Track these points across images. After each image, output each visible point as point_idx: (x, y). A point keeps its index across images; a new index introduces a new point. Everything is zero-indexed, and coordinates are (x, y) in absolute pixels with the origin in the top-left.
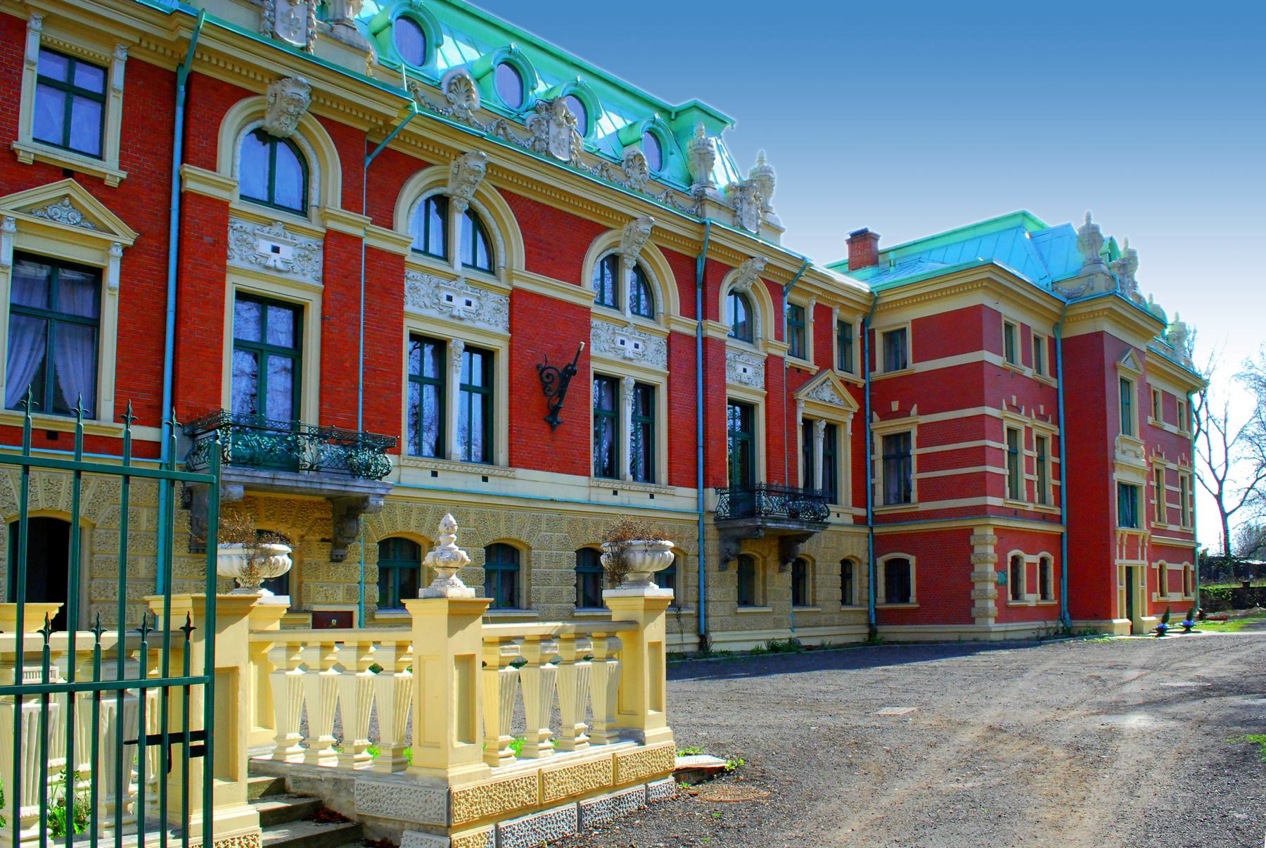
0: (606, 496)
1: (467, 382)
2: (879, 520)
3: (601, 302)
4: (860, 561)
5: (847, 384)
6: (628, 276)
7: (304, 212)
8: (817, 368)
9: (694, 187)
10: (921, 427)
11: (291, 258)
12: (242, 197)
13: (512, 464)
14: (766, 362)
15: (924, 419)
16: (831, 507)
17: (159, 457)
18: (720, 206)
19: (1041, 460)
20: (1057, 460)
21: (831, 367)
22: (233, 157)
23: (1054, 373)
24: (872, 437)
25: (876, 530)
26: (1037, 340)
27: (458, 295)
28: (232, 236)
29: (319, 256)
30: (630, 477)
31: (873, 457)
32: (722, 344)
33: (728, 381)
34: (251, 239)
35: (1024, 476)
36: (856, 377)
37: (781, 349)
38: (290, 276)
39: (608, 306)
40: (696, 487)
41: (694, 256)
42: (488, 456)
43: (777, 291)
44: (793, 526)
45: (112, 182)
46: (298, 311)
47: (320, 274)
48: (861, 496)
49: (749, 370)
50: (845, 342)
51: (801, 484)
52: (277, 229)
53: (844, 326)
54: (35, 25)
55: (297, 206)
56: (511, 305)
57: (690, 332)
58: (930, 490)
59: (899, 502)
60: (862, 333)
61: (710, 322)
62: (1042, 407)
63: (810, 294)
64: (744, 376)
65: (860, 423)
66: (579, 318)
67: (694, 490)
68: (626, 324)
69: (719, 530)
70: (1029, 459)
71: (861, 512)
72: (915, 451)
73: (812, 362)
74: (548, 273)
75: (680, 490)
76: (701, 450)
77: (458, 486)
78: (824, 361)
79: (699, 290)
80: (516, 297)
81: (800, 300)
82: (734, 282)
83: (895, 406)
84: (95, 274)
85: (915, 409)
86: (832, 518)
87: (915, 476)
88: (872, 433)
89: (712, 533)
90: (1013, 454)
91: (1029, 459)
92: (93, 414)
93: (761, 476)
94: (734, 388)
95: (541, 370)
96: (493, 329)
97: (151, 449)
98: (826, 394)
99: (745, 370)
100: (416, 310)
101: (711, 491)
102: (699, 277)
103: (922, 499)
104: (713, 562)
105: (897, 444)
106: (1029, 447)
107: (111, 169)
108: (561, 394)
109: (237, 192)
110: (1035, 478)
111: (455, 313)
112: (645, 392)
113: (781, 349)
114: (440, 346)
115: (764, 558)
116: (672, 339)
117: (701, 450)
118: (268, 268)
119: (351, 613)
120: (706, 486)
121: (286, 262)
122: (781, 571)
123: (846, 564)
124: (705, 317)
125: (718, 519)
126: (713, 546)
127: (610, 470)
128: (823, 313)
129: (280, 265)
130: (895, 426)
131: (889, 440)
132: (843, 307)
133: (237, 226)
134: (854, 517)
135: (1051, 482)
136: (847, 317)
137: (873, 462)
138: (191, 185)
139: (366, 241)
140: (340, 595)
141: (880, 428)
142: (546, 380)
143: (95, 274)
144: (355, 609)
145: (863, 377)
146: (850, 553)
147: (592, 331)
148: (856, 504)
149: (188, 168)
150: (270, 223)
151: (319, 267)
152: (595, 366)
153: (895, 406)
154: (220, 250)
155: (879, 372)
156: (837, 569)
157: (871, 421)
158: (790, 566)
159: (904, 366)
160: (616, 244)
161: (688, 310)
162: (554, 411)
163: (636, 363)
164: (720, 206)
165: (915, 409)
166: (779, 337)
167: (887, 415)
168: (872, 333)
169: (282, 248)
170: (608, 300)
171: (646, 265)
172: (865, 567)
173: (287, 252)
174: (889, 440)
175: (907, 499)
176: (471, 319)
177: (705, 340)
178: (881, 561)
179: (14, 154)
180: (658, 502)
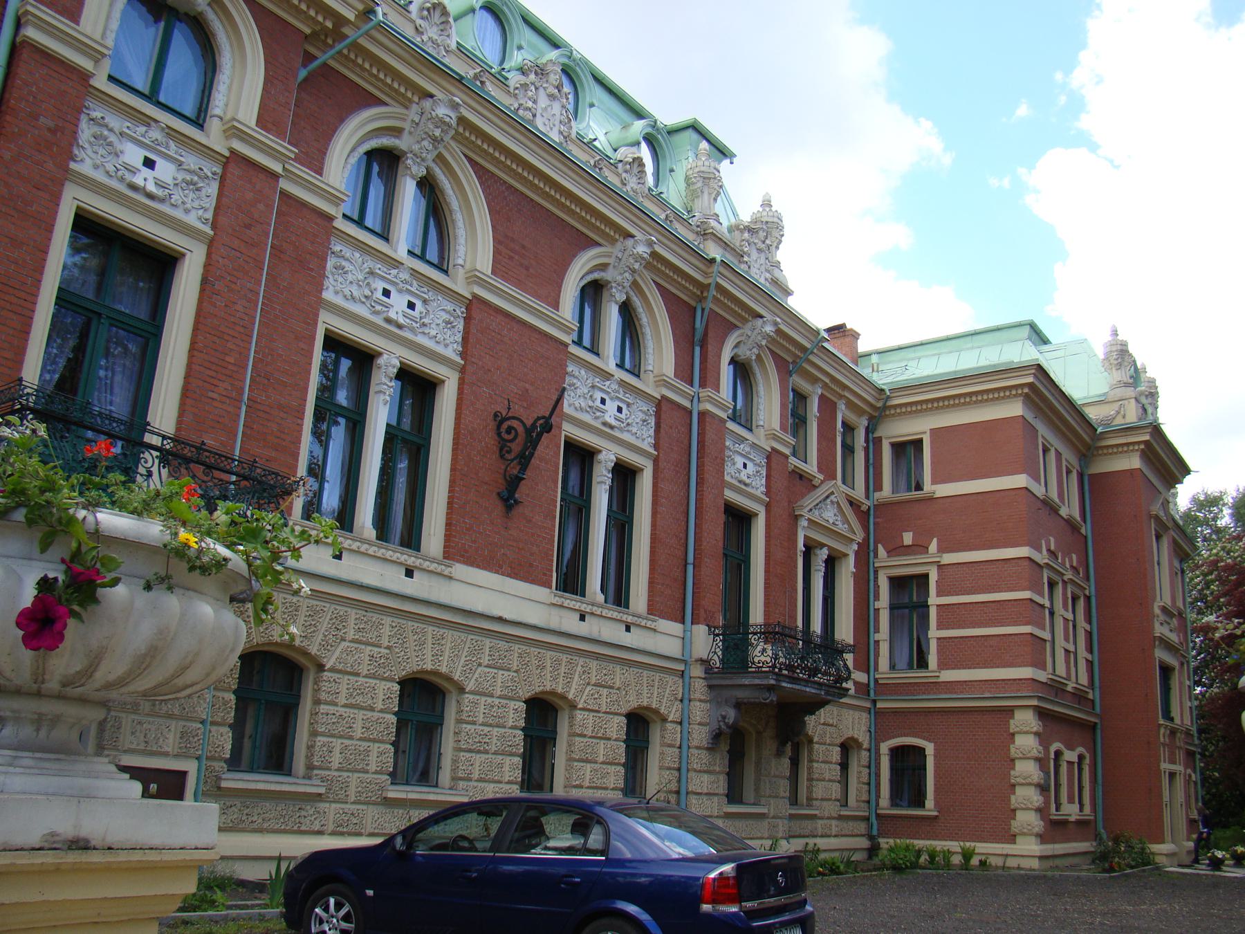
0: (570, 623)
1: (394, 423)
3: (579, 343)
5: (852, 503)
7: (198, 121)
8: (821, 477)
11: (170, 181)
12: (111, 78)
15: (948, 558)
20: (1088, 627)
21: (834, 478)
22: (108, 17)
24: (876, 578)
25: (879, 705)
26: (1069, 472)
27: (400, 291)
28: (86, 132)
29: (213, 189)
30: (600, 598)
31: (877, 605)
34: (112, 138)
35: (1060, 642)
39: (585, 348)
40: (683, 622)
41: (693, 303)
42: (411, 539)
43: (784, 369)
46: (159, 265)
47: (209, 215)
50: (848, 449)
51: (817, 626)
52: (155, 134)
53: (848, 428)
55: (189, 110)
56: (468, 320)
58: (955, 654)
59: (910, 667)
60: (867, 441)
63: (815, 380)
64: (744, 475)
65: (864, 556)
67: (680, 626)
69: (710, 687)
72: (933, 600)
73: (815, 469)
74: (519, 284)
75: (665, 625)
76: (690, 569)
79: (697, 350)
80: (475, 310)
81: (804, 386)
82: (736, 346)
85: (933, 547)
87: (934, 633)
88: (876, 572)
93: (757, 615)
95: (499, 420)
96: (440, 349)
98: (829, 515)
99: (745, 466)
100: (339, 301)
101: (701, 630)
103: (943, 665)
105: (909, 589)
108: (525, 460)
109: (106, 68)
111: (392, 315)
112: (624, 475)
114: (364, 359)
115: (759, 733)
117: (690, 569)
118: (133, 187)
119: (184, 774)
121: (159, 184)
122: (779, 754)
124: (703, 385)
127: (572, 582)
129: (151, 187)
130: (907, 566)
131: (899, 583)
132: (850, 405)
133: (97, 114)
136: (852, 418)
137: (877, 611)
139: (284, 184)
140: (171, 741)
141: (887, 565)
142: (506, 437)
144: (191, 767)
145: (867, 497)
146: (850, 734)
147: (568, 379)
150: (148, 121)
151: (211, 204)
152: (569, 430)
153: (908, 538)
154: (61, 145)
155: (887, 491)
157: (876, 556)
158: (789, 747)
159: (919, 487)
160: (603, 267)
161: (684, 371)
162: (514, 483)
163: (617, 433)
166: (783, 428)
167: (897, 550)
168: (878, 441)
169: (160, 163)
170: (587, 341)
171: (637, 302)
173: (165, 170)
174: (899, 583)
175: (923, 663)
176: (412, 330)
178: (885, 748)
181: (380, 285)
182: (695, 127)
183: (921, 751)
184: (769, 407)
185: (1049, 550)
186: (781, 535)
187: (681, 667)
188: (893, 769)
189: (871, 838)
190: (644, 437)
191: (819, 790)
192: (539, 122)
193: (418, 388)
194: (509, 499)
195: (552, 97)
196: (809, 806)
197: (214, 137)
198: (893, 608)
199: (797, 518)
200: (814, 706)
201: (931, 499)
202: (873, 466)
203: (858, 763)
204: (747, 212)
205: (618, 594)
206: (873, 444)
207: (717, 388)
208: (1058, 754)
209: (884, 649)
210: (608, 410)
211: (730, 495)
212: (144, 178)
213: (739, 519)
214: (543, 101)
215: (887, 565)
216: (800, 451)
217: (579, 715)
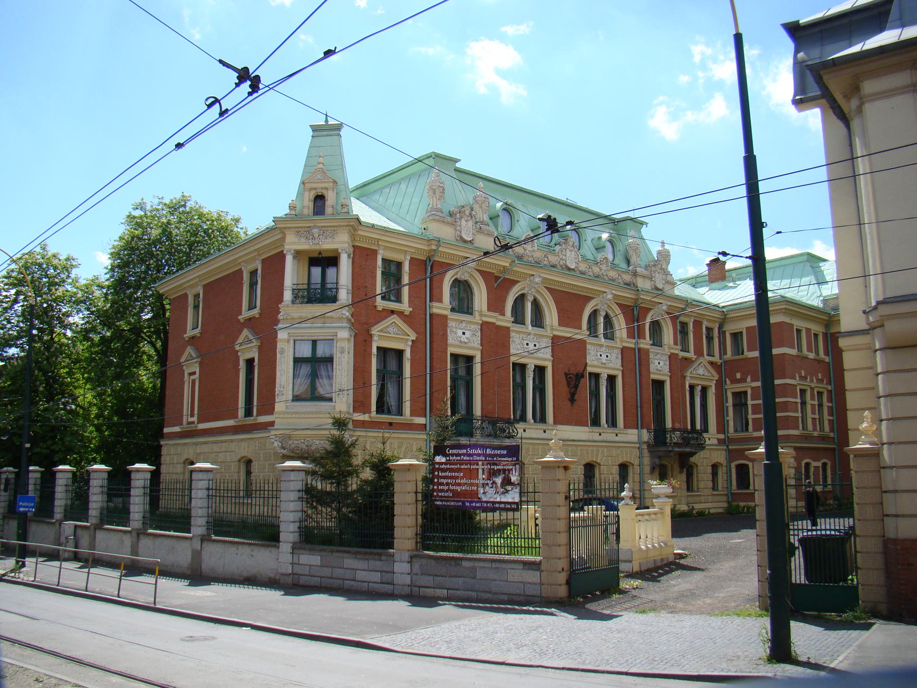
2: (731, 441)
4: (722, 465)
5: (711, 363)
6: (601, 320)
9: (631, 268)
10: (752, 388)
13: (556, 422)
14: (670, 357)
16: (705, 435)
18: (644, 277)
19: (820, 405)
20: (830, 405)
23: (826, 353)
30: (606, 426)
32: (647, 352)
36: (716, 359)
37: (677, 350)
38: (469, 344)
42: (543, 420)
43: (674, 319)
44: (687, 450)
45: (407, 313)
48: (722, 427)
49: (662, 363)
50: (710, 339)
52: (464, 325)
53: (709, 330)
54: (381, 252)
57: (633, 346)
60: (719, 333)
61: (642, 341)
62: (820, 375)
64: (659, 367)
65: (720, 385)
66: (581, 346)
68: (602, 346)
70: (813, 406)
71: (721, 436)
72: (750, 402)
77: (535, 436)
78: (698, 352)
83: (738, 376)
84: (400, 353)
85: (749, 379)
86: (708, 442)
89: (646, 453)
90: (803, 403)
91: (813, 406)
92: (400, 412)
94: (654, 373)
98: (701, 371)
101: (645, 431)
102: (634, 312)
103: (755, 430)
104: (647, 469)
106: (812, 398)
107: (405, 306)
110: (817, 416)
113: (677, 350)
114: (523, 367)
116: (624, 350)
122: (681, 472)
123: (715, 467)
124: (639, 337)
125: (649, 446)
126: (647, 460)
127: (596, 422)
128: (698, 324)
130: (739, 387)
131: (736, 395)
132: (708, 320)
134: (718, 439)
135: (826, 417)
136: (710, 325)
138: (435, 311)
141: (731, 388)
143: (400, 353)
148: (718, 432)
149: (435, 304)
151: (479, 339)
153: (738, 376)
156: (709, 469)
158: (685, 470)
159: (743, 354)
161: (631, 335)
162: (573, 395)
163: (607, 366)
164: (644, 277)
165: (749, 379)
166: (676, 343)
167: (734, 381)
171: (610, 312)
172: (724, 468)
173: (468, 333)
174: (736, 395)
175: (747, 430)
177: (639, 349)
178: (733, 465)
179: (375, 307)
180: (620, 438)
181: (525, 342)
183: (748, 465)
184: (668, 334)
185: (801, 377)
188: (737, 473)
189: (729, 502)
190: (617, 363)
191: (702, 485)
192: (569, 265)
193: (540, 371)
194: (572, 400)
195: (571, 251)
196: (698, 491)
197: (477, 318)
198: (734, 405)
199: (685, 377)
200: (692, 454)
201: (747, 359)
202: (722, 344)
203: (721, 473)
204: (655, 248)
205: (613, 423)
206: (722, 334)
207: (645, 339)
208: (807, 465)
209: (731, 423)
210: (603, 358)
211: (653, 376)
212: (464, 339)
213: (658, 385)
214: (568, 253)
215: (731, 388)
216: (685, 349)
217: (602, 467)
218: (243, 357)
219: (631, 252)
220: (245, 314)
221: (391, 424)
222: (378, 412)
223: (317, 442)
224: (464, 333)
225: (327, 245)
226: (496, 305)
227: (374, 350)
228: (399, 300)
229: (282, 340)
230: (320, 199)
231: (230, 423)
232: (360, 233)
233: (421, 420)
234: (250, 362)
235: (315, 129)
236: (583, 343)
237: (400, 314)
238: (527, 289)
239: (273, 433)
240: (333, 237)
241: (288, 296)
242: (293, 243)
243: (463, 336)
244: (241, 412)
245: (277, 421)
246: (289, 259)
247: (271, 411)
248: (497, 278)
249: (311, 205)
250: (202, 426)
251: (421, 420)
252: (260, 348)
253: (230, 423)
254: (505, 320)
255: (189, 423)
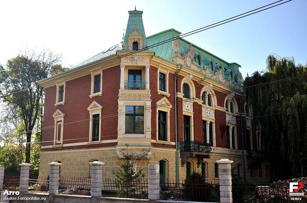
17: (175, 148)
33: (247, 126)
45: (168, 96)
47: (193, 110)
80: (216, 111)
97: (174, 147)
107: (167, 93)
120: (244, 150)
124: (242, 112)
127: (229, 147)
151: (193, 109)
182: (235, 64)
186: (254, 134)
187: (243, 157)
218: (91, 114)
219: (238, 77)
220: (92, 95)
221: (163, 144)
222: (159, 139)
223: (138, 152)
224: (188, 106)
225: (140, 64)
226: (198, 96)
227: (157, 112)
228: (165, 90)
229: (121, 106)
230: (136, 44)
231: (85, 143)
232: (153, 59)
233: (173, 143)
234: (96, 116)
235: (130, 12)
236: (225, 113)
237: (166, 96)
238: (207, 89)
239: (117, 147)
240: (142, 61)
241: (122, 85)
242: (125, 63)
243: (188, 109)
244: (90, 139)
245: (119, 142)
246: (123, 70)
247: (116, 138)
248: (198, 84)
249: (132, 45)
250: (65, 145)
251: (173, 143)
252: (102, 110)
253: (85, 143)
254: (200, 102)
255: (56, 144)
